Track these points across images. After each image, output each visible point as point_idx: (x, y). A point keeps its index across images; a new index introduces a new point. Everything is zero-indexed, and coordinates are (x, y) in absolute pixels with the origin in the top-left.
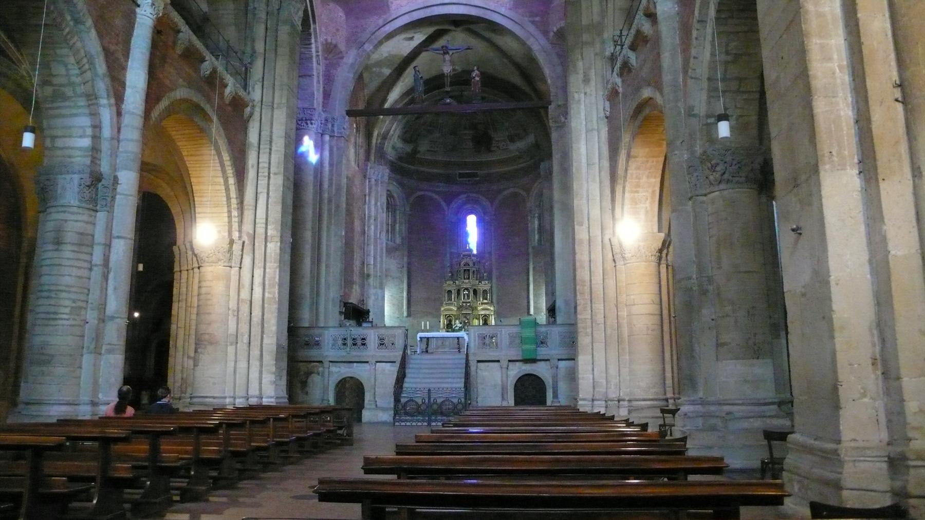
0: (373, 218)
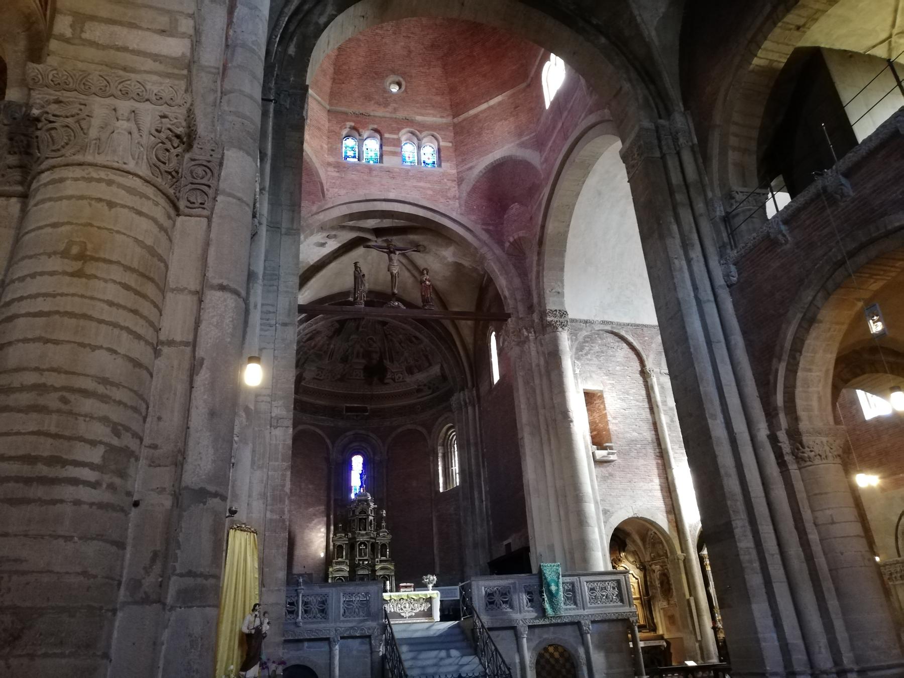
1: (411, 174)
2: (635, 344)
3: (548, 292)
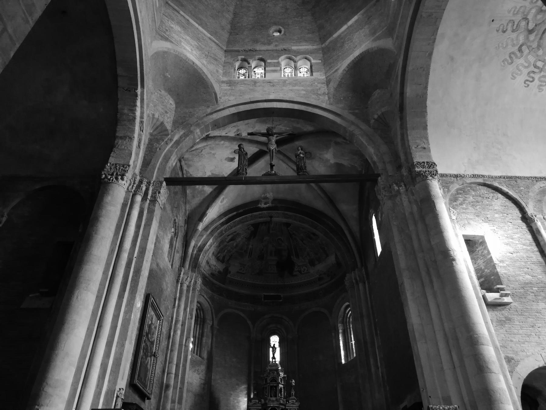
0: (180, 323)
1: (287, 82)
2: (511, 193)
3: (413, 148)
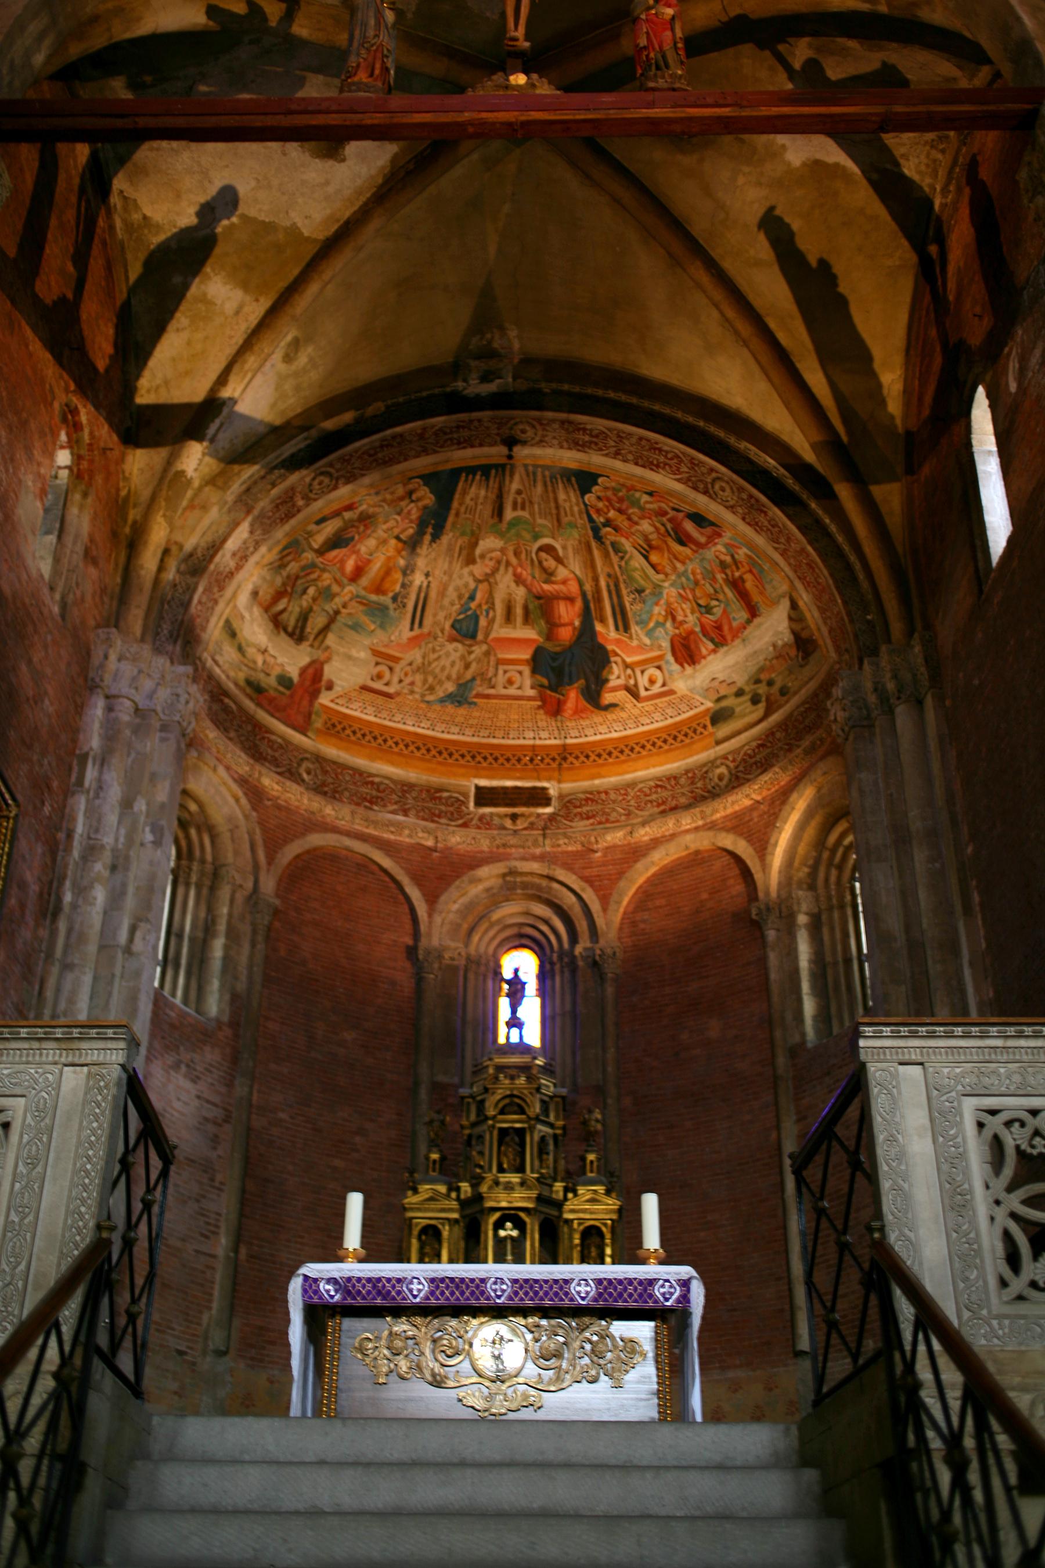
0: (107, 856)
